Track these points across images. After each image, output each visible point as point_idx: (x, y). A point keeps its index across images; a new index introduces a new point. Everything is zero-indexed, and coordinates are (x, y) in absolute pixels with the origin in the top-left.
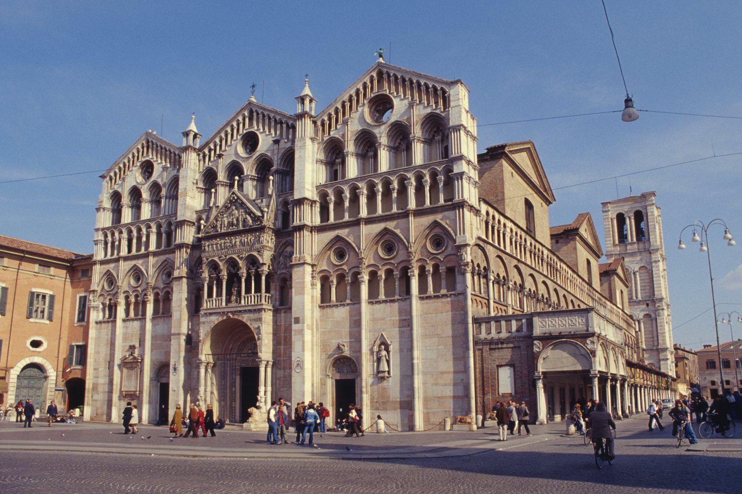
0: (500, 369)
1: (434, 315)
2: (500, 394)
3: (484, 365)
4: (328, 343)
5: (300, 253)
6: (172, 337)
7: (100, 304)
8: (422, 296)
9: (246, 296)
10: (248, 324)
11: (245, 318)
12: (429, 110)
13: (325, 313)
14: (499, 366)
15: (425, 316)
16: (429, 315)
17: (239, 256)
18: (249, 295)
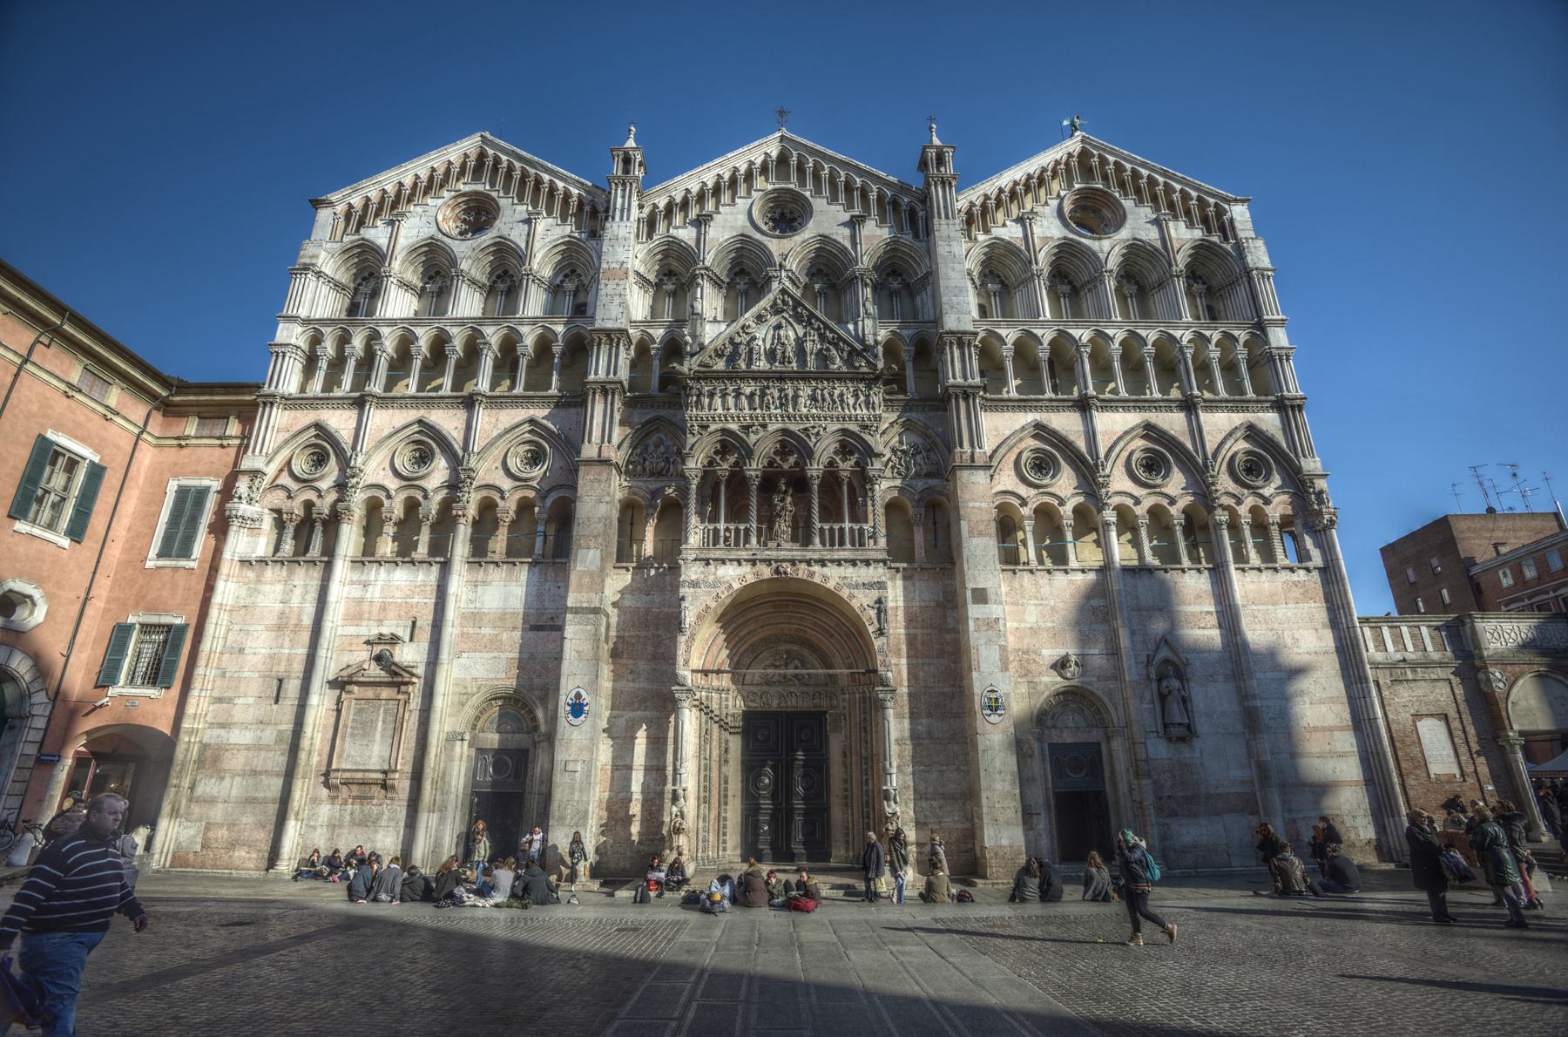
0: (1418, 723)
1: (1270, 607)
2: (1433, 776)
3: (1391, 716)
4: (1033, 656)
5: (972, 445)
6: (569, 616)
7: (266, 511)
8: (1241, 566)
9: (826, 527)
10: (845, 593)
11: (831, 577)
12: (1198, 234)
13: (1017, 585)
14: (1418, 716)
15: (1254, 607)
16: (1261, 607)
17: (806, 429)
18: (836, 527)
